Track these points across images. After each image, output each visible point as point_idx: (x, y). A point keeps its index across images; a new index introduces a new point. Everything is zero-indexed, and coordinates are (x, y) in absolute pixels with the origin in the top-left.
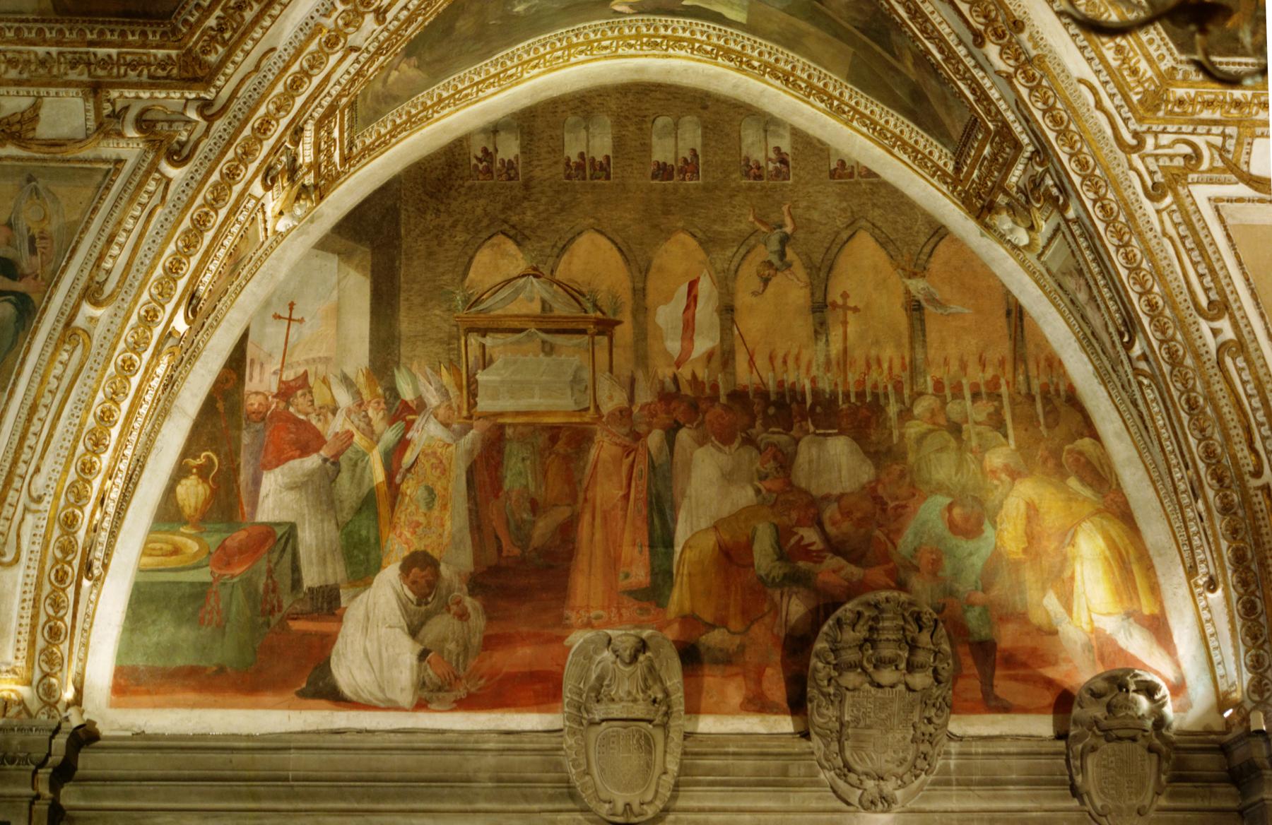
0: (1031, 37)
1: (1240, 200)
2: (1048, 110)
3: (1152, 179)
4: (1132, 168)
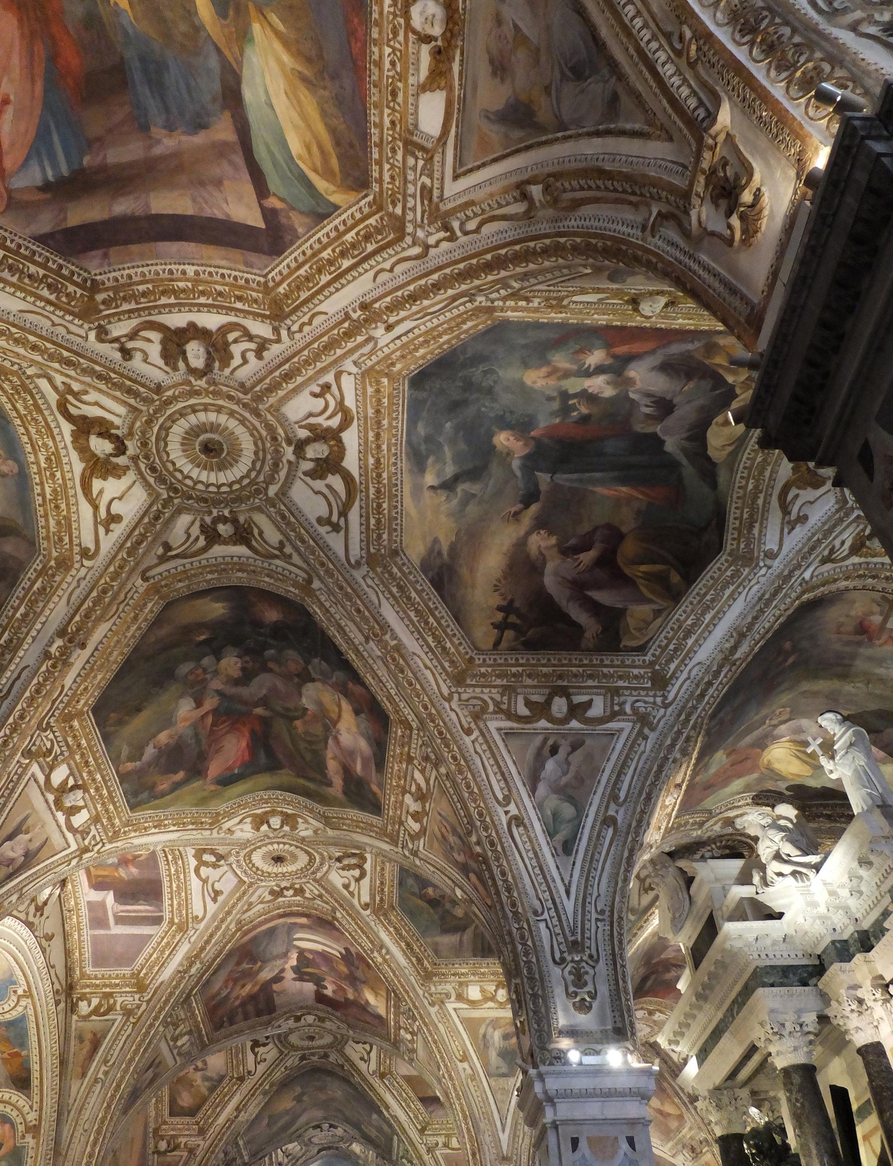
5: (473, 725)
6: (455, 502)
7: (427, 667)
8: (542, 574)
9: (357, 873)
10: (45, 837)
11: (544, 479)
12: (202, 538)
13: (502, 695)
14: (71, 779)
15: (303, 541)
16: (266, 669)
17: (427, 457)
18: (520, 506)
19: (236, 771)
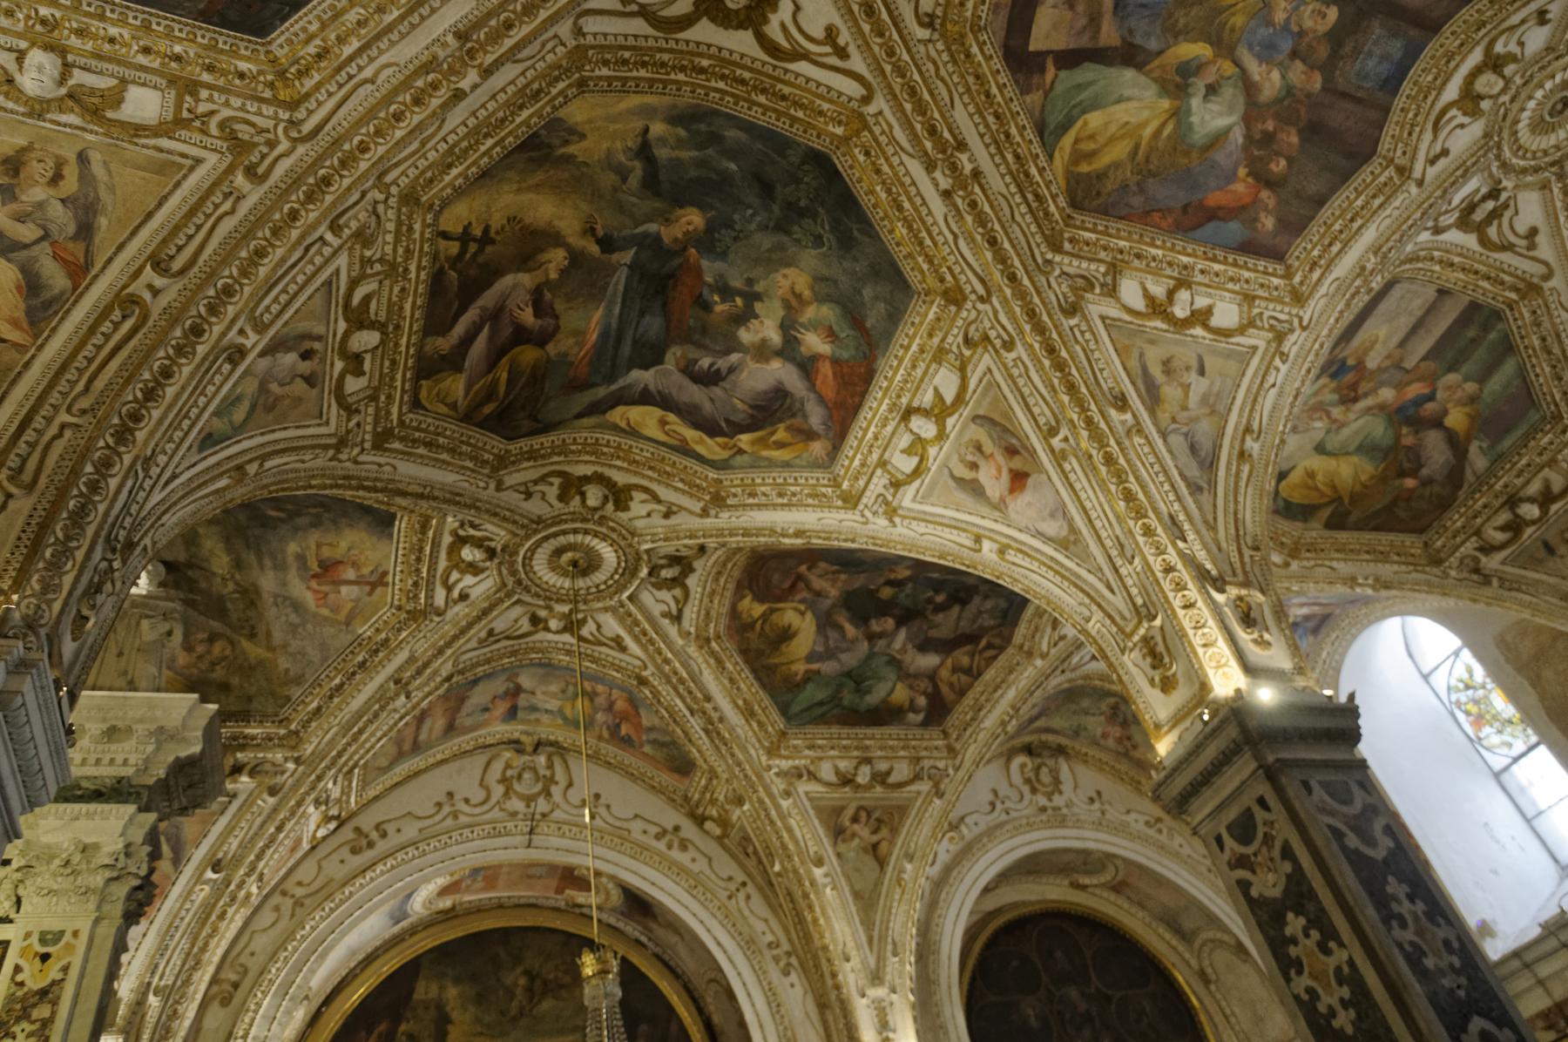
5: (347, 231)
6: (622, 158)
7: (423, 144)
8: (519, 270)
11: (627, 257)
13: (381, 260)
17: (687, 129)
18: (600, 233)
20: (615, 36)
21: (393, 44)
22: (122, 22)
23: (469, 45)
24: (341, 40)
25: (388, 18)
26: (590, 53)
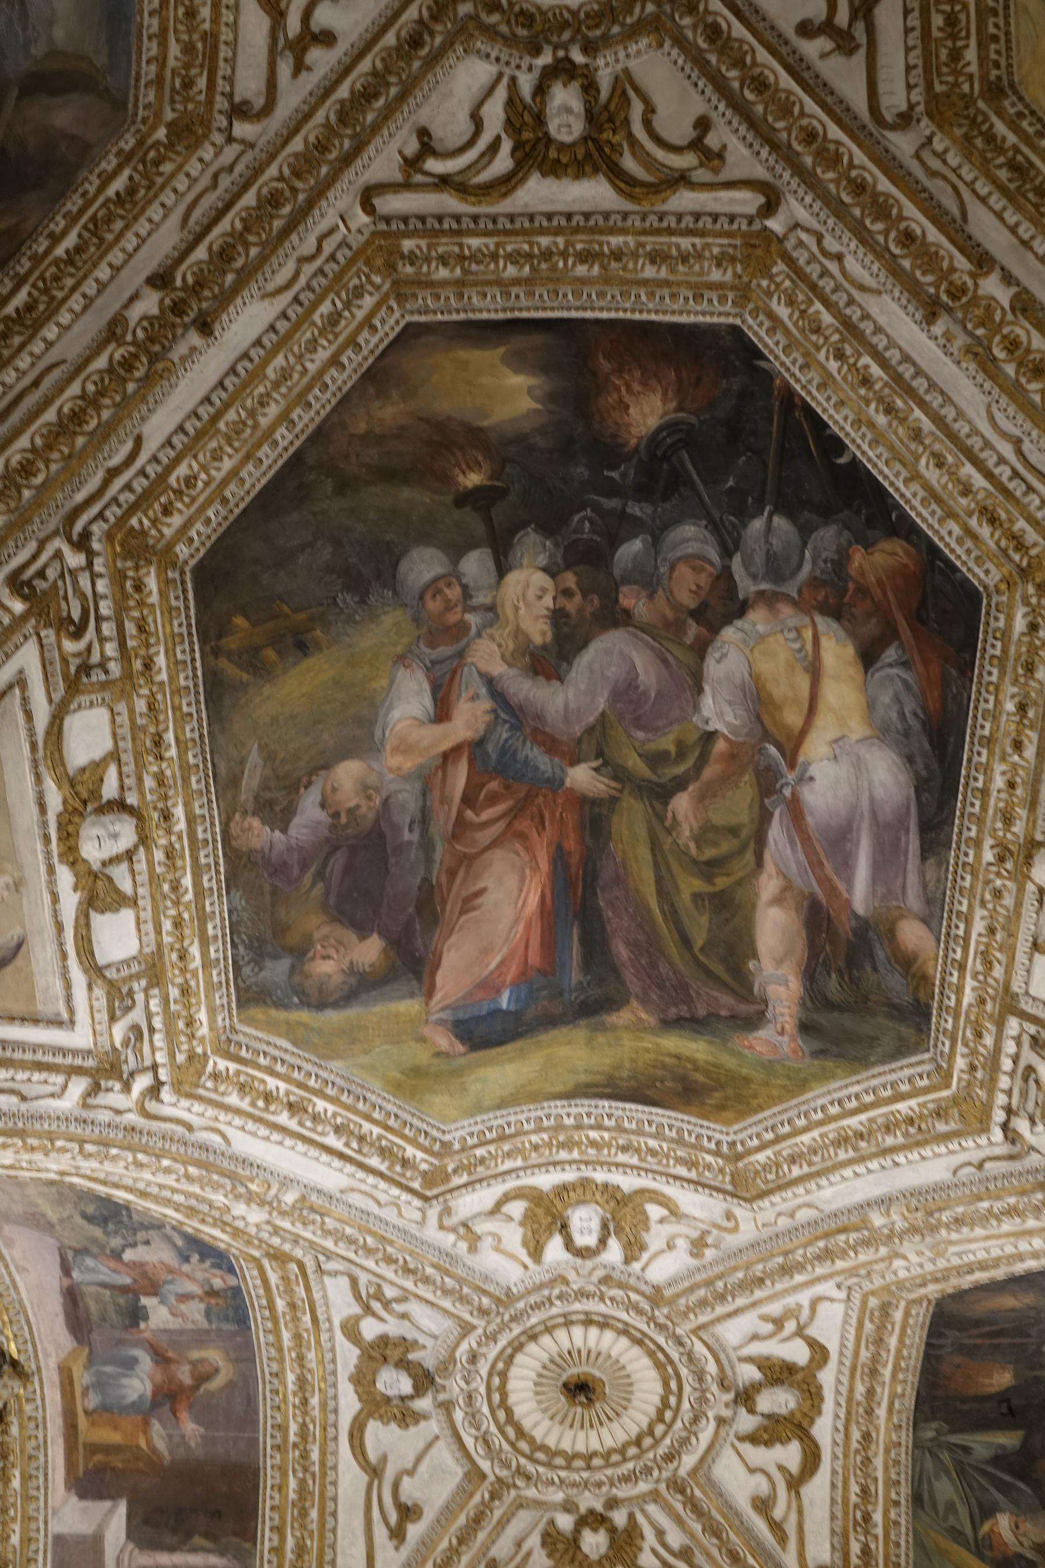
0: (193, 350)
1: (29, 715)
2: (91, 402)
3: (32, 578)
4: (42, 545)
9: (791, 1454)
10: (16, 932)
12: (506, 146)
14: (112, 772)
15: (761, 85)
16: (615, 617)
19: (504, 1001)
20: (908, 50)
21: (960, 414)
22: (987, 769)
23: (944, 298)
24: (967, 490)
25: (927, 425)
26: (939, 88)
